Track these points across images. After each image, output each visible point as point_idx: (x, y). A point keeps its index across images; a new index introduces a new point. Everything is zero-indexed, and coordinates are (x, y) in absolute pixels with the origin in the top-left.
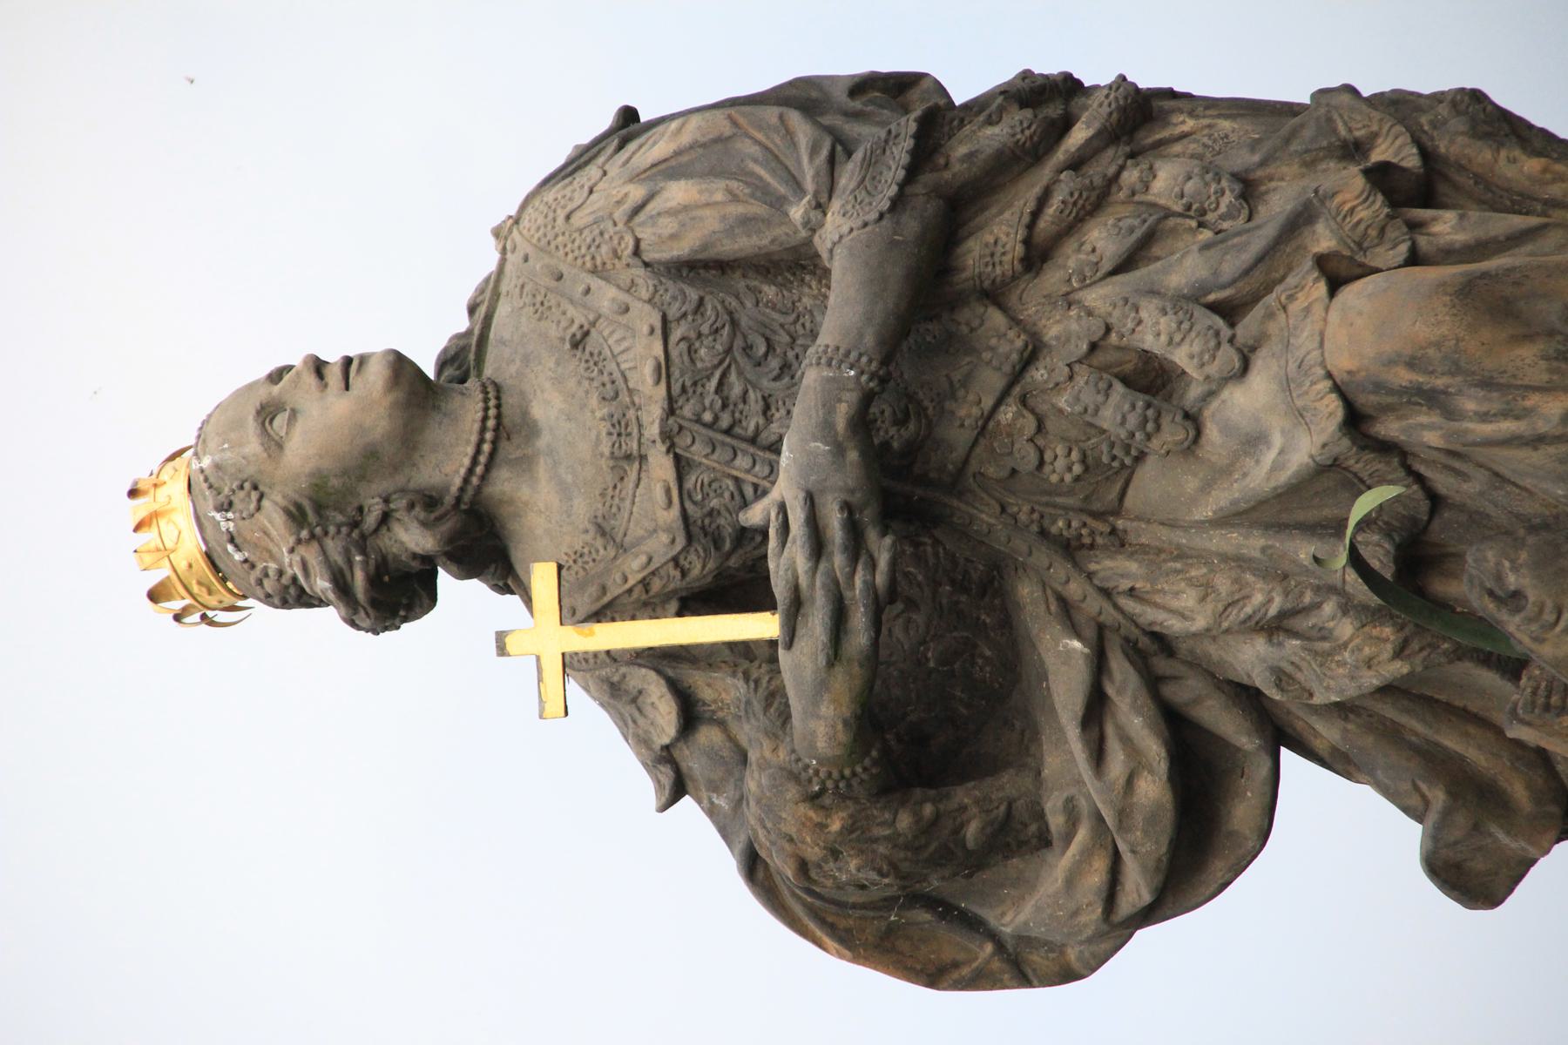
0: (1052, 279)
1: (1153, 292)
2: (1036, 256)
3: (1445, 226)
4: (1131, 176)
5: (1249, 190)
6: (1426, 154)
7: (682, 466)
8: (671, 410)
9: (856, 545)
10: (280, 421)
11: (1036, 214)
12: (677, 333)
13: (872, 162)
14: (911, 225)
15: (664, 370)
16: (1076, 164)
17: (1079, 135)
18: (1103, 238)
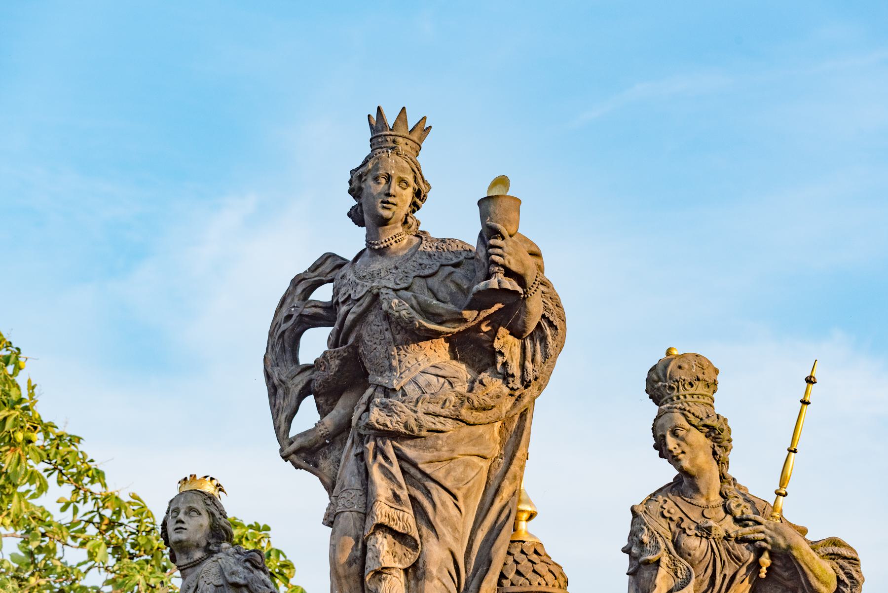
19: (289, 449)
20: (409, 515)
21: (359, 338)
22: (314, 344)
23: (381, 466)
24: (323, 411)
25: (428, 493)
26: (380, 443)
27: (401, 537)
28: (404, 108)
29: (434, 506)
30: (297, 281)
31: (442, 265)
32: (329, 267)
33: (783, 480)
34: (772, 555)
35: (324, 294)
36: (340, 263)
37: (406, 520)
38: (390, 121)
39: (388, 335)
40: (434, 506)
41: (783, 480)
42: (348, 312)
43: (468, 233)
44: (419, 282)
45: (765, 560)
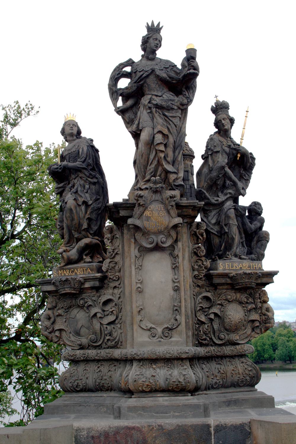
0: (80, 179)
1: (78, 187)
2: (81, 178)
3: (83, 208)
4: (87, 183)
5: (87, 192)
6: (91, 204)
7: (67, 155)
8: (70, 153)
9: (60, 168)
10: (69, 125)
11: (83, 177)
12: (74, 153)
13: (81, 164)
14: (77, 168)
15: (72, 152)
16: (87, 179)
17: (89, 179)
18: (82, 182)
19: (118, 110)
20: (167, 130)
21: (145, 82)
22: (124, 83)
23: (158, 115)
24: (124, 101)
25: (170, 124)
26: (157, 110)
27: (164, 135)
28: (159, 22)
29: (172, 128)
30: (121, 65)
31: (170, 66)
32: (130, 62)
33: (243, 136)
34: (241, 154)
35: (128, 69)
36: (133, 62)
37: (166, 131)
38: (150, 25)
39: (156, 82)
40: (172, 128)
41: (243, 136)
42: (143, 74)
43: (177, 59)
44: (164, 69)
45: (239, 155)
